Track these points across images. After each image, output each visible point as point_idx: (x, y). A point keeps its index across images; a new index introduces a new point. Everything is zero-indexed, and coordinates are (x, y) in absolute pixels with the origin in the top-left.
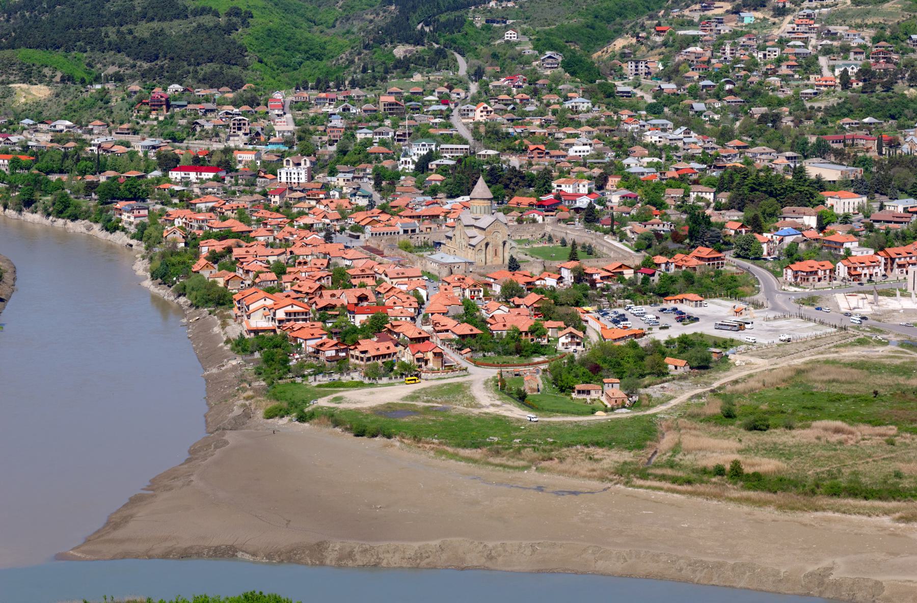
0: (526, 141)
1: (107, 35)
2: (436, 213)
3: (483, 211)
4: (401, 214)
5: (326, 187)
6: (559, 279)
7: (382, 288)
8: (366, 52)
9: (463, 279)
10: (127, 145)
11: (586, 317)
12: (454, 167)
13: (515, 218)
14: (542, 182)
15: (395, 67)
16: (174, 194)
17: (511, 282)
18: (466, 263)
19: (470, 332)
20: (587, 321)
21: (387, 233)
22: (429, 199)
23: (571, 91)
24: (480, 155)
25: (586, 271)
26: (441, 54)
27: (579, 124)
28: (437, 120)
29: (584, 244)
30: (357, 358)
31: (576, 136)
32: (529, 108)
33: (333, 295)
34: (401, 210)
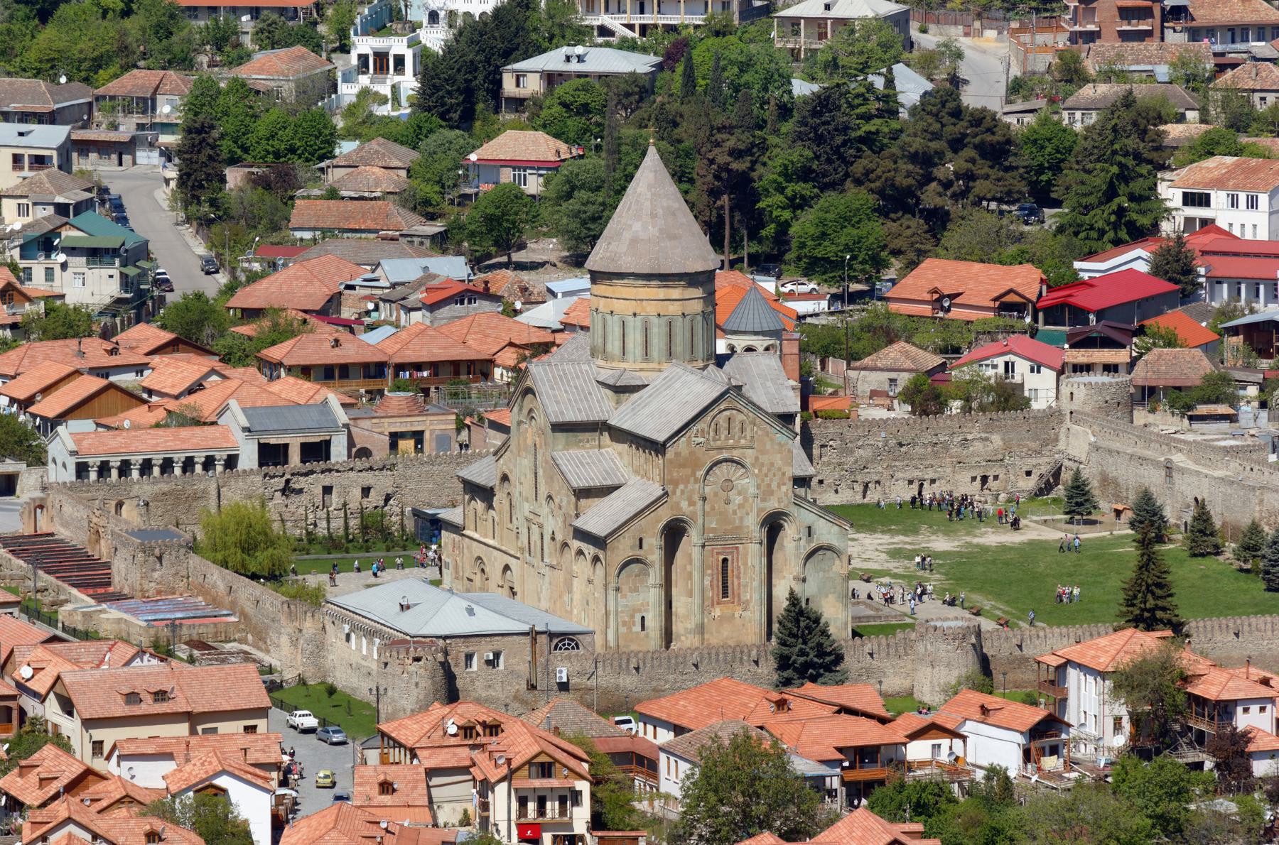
2: (475, 349)
3: (658, 343)
4: (275, 353)
6: (1036, 732)
7: (33, 777)
9: (494, 729)
13: (904, 379)
14: (1099, 180)
18: (533, 635)
21: (167, 465)
22: (453, 268)
24: (795, 22)
25: (1198, 690)
29: (1255, 529)
34: (281, 333)
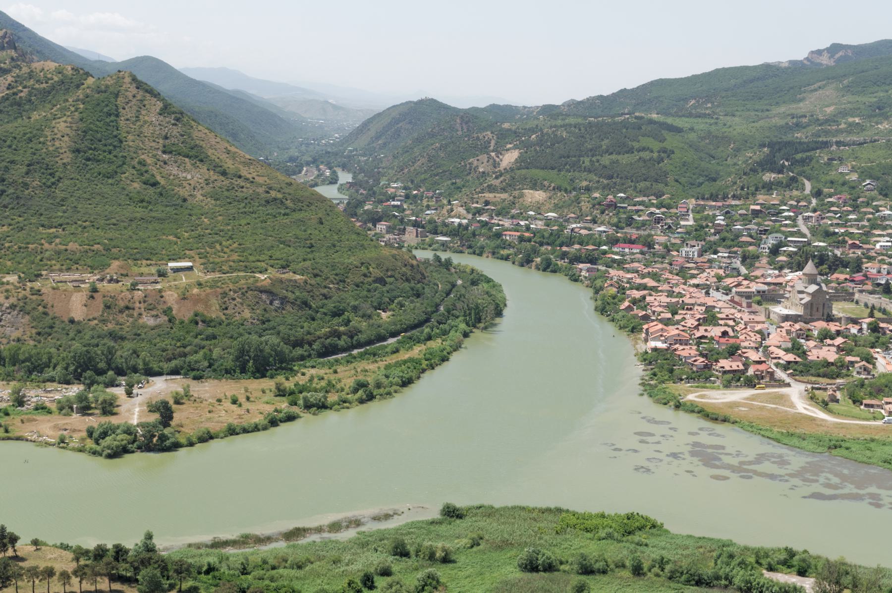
0: (847, 238)
1: (584, 163)
5: (710, 261)
8: (744, 177)
10: (590, 229)
11: (876, 355)
12: (795, 253)
15: (763, 187)
16: (614, 261)
17: (826, 329)
19: (793, 360)
20: (876, 359)
22: (777, 272)
23: (881, 206)
26: (793, 180)
27: (884, 228)
28: (787, 222)
30: (717, 371)
31: (883, 236)
32: (850, 217)
33: (706, 330)
